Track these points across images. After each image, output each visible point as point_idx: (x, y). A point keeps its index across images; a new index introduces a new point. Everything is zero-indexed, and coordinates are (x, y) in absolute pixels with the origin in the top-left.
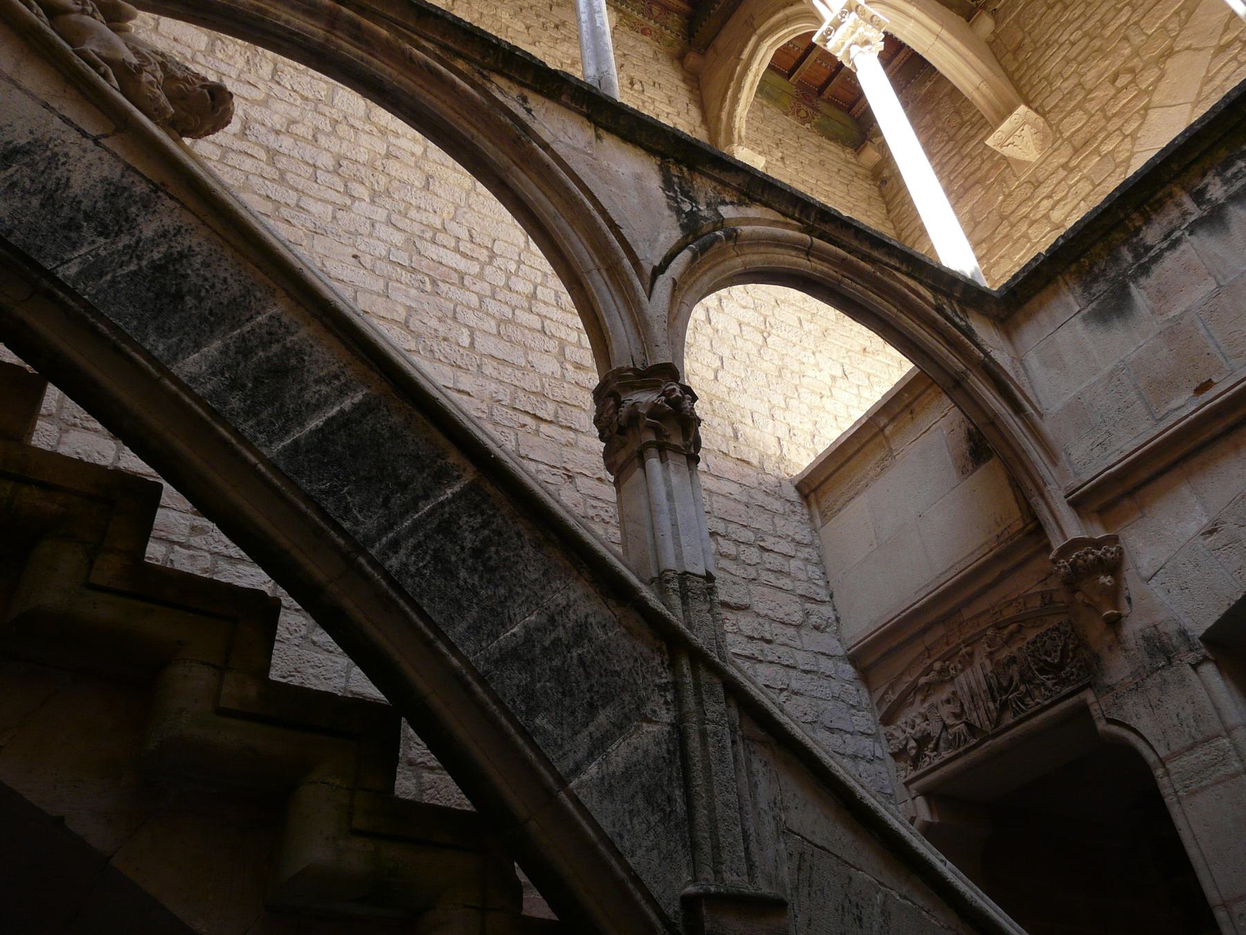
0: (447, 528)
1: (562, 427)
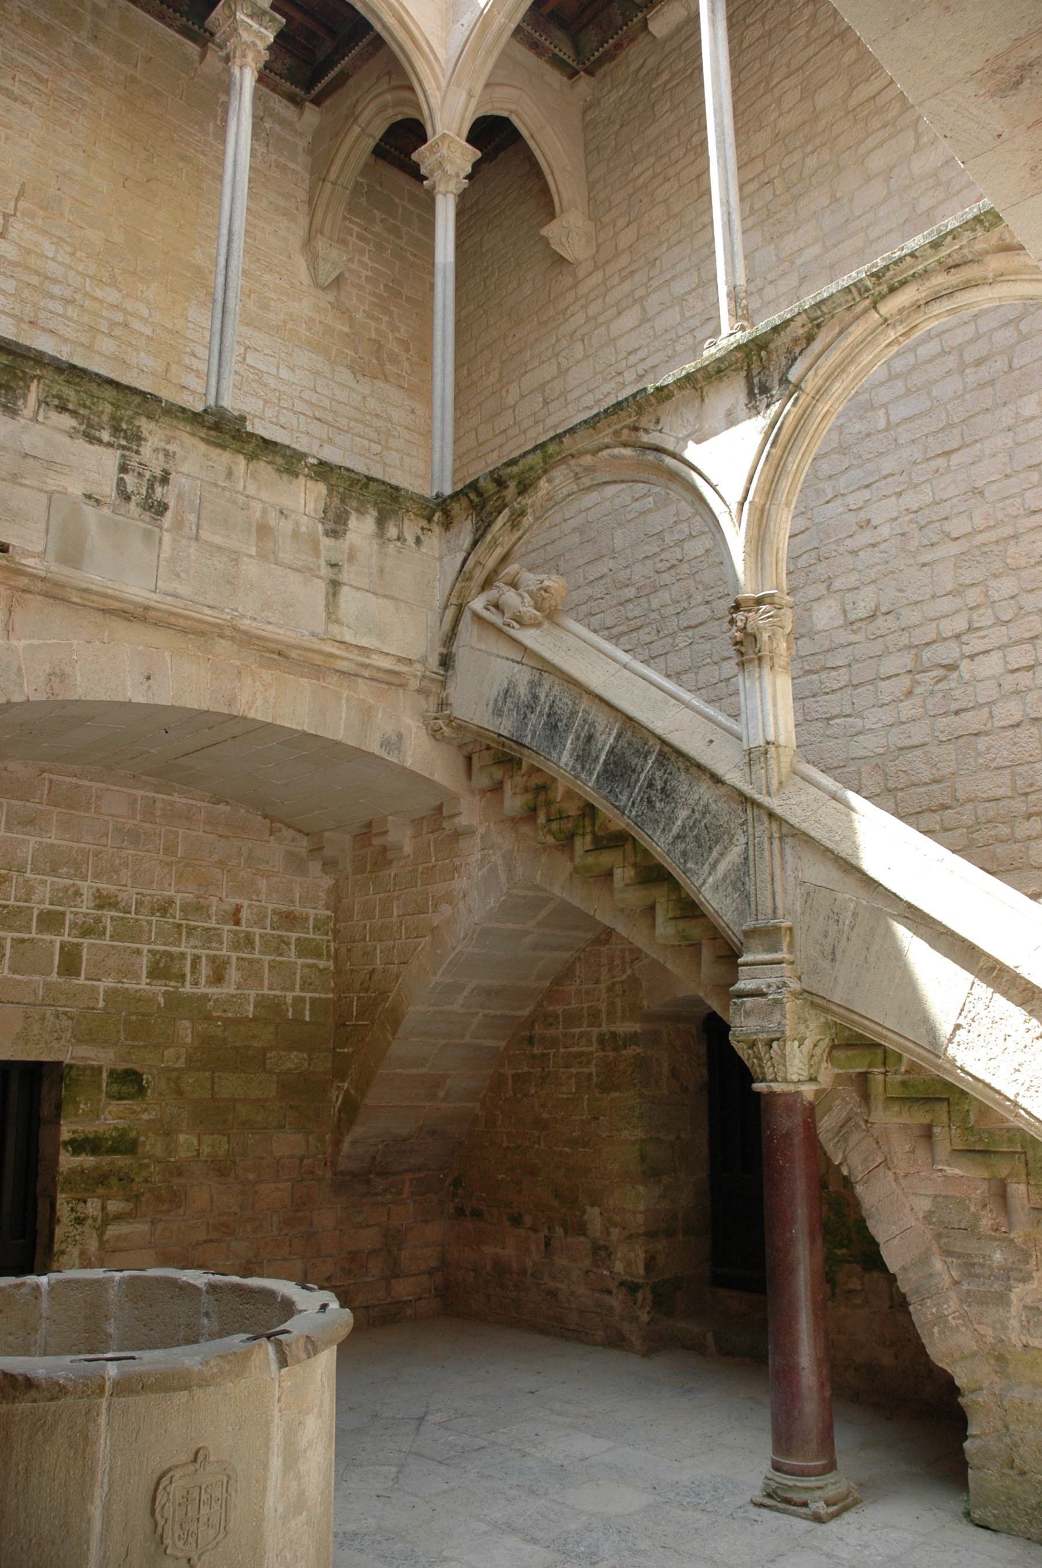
0: (650, 785)
1: (969, 446)
